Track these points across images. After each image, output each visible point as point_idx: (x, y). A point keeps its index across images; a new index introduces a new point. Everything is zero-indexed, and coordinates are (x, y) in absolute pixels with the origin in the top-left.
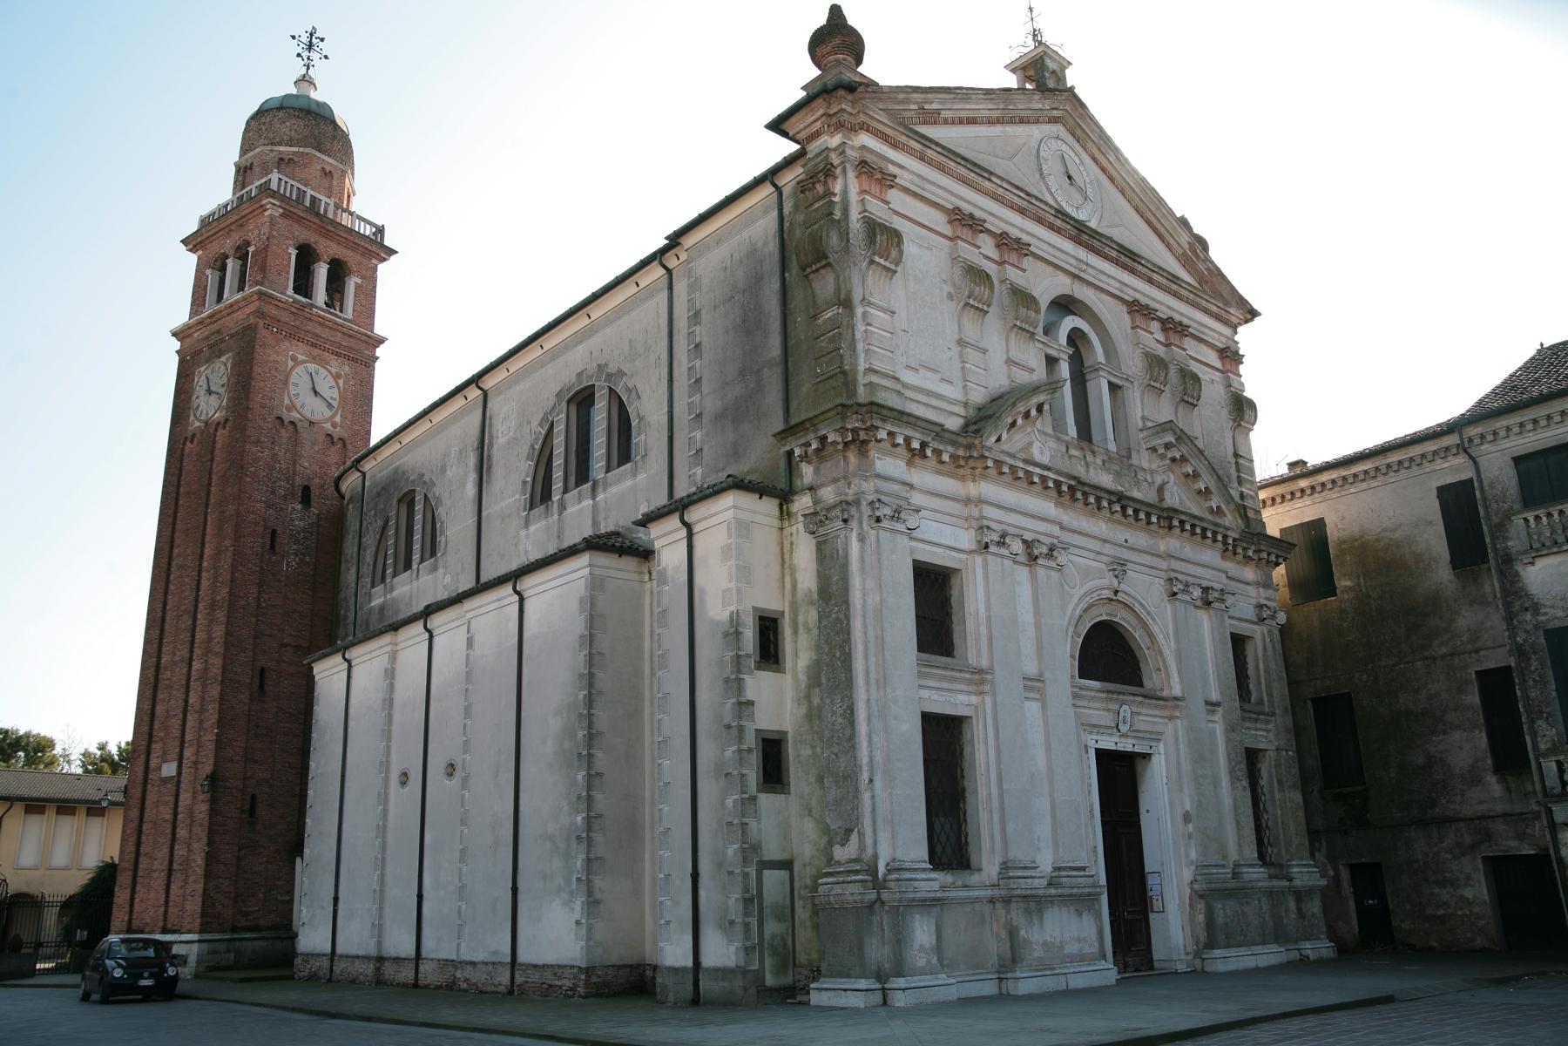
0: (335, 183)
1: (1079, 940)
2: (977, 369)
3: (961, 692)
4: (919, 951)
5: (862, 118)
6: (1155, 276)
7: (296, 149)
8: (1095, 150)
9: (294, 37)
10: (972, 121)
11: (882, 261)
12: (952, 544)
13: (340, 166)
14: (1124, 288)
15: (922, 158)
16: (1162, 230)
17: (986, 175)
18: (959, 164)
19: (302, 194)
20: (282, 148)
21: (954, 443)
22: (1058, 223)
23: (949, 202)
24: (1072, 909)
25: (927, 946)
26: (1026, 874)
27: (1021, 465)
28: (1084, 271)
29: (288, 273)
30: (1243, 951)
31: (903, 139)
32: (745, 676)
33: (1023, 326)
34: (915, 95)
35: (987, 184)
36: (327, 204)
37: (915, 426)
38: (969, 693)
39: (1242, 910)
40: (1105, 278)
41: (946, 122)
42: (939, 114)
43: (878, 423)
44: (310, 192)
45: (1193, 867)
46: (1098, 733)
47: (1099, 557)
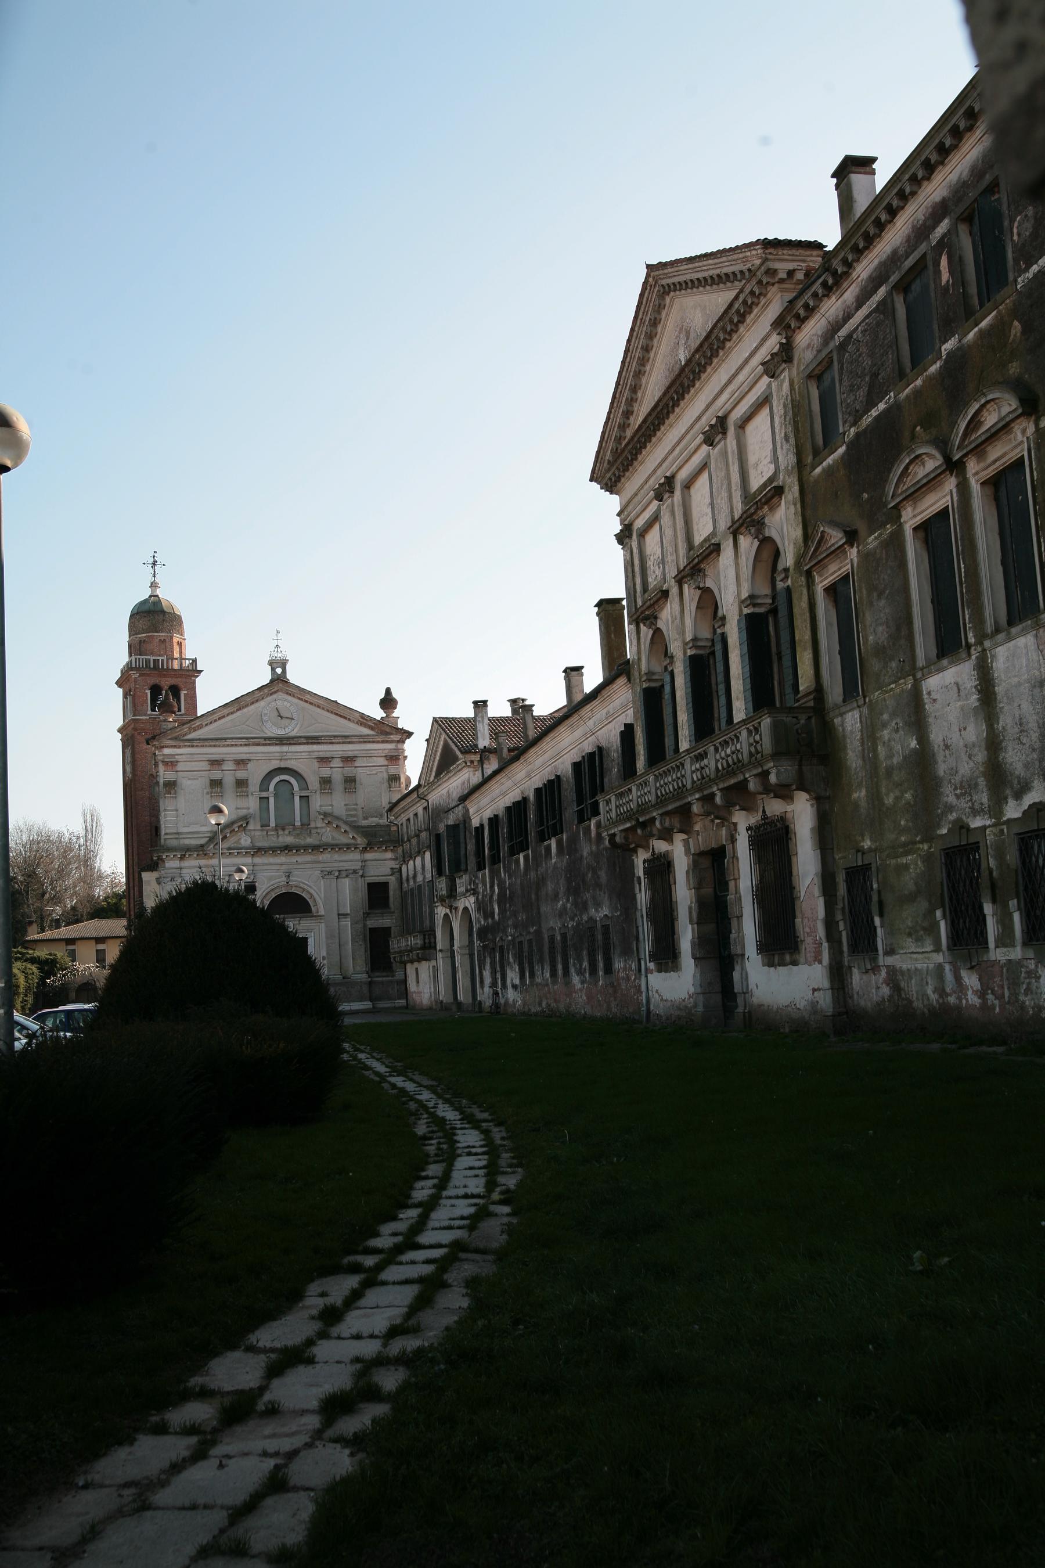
0: (167, 644)
7: (145, 635)
9: (144, 564)
10: (223, 717)
13: (169, 634)
14: (312, 754)
19: (148, 661)
20: (140, 636)
22: (268, 742)
29: (147, 703)
31: (182, 744)
35: (226, 743)
36: (162, 660)
37: (176, 851)
40: (299, 754)
41: (207, 725)
44: (152, 658)
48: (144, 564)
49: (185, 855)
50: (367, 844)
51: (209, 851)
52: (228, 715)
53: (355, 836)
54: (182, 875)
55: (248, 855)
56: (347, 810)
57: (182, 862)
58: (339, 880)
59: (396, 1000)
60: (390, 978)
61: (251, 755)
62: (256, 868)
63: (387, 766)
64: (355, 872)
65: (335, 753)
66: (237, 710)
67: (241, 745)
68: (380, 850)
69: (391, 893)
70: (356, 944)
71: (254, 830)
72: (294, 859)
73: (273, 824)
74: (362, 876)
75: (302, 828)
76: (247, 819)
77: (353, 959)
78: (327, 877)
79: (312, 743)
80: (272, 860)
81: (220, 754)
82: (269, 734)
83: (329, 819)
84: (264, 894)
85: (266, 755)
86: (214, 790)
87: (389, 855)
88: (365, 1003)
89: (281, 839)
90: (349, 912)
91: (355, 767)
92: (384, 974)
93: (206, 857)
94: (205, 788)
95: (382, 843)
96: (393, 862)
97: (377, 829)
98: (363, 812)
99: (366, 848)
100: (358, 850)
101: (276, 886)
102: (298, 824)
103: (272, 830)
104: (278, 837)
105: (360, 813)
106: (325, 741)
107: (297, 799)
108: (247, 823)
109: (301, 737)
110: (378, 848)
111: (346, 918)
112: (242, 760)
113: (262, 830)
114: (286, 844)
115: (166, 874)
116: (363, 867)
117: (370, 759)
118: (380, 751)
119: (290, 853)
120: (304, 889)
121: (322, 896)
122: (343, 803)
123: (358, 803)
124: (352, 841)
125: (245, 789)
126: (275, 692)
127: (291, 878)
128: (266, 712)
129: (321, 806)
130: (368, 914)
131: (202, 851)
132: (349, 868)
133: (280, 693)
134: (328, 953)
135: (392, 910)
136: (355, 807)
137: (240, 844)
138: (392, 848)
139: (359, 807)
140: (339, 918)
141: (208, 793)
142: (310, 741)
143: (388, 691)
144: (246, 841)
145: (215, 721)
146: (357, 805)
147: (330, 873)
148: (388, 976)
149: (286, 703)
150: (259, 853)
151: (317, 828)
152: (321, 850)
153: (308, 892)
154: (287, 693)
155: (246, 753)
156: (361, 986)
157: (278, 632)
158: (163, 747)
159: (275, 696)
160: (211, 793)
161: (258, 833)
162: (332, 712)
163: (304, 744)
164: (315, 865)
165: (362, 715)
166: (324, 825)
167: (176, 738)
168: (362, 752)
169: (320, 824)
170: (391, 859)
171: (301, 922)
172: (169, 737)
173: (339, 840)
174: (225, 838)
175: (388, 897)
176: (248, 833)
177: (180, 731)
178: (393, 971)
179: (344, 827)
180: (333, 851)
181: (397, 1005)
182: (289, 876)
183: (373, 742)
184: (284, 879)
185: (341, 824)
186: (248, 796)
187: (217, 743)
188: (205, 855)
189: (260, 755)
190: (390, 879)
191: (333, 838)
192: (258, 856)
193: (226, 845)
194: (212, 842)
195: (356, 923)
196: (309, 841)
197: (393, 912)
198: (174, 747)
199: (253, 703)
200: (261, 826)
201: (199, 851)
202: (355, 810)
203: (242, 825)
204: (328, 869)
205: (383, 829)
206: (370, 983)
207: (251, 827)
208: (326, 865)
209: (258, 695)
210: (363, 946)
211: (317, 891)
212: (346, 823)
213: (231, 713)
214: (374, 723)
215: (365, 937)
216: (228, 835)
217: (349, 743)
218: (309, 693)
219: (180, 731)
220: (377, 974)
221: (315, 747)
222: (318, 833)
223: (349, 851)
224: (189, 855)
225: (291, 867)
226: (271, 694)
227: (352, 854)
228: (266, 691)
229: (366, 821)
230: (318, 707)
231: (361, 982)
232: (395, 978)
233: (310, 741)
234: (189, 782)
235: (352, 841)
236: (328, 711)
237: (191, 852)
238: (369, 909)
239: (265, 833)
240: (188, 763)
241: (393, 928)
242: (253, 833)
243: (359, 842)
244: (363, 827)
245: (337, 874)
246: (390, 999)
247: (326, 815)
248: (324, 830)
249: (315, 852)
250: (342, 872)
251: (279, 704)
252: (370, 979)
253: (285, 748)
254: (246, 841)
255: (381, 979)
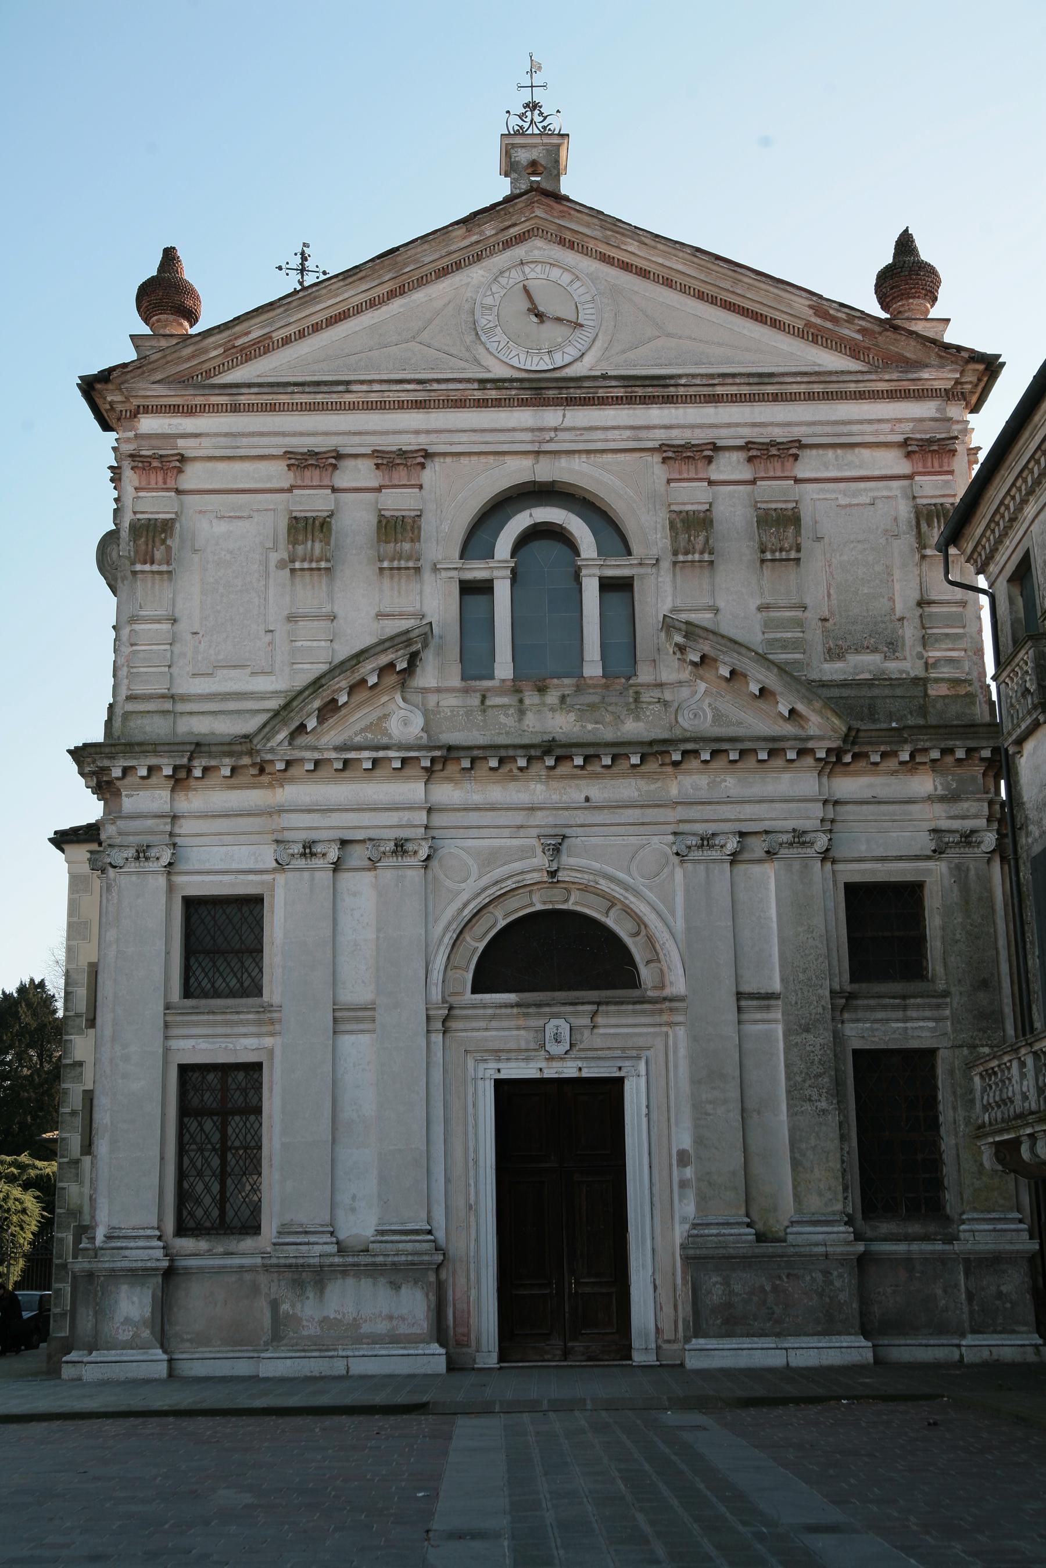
1: (391, 1318)
2: (315, 644)
3: (245, 1035)
4: (122, 1324)
5: (135, 402)
6: (719, 390)
8: (603, 248)
9: (280, 268)
11: (147, 567)
12: (251, 866)
14: (643, 434)
15: (235, 409)
16: (757, 308)
17: (341, 388)
18: (293, 393)
21: (230, 754)
22: (493, 394)
23: (277, 445)
24: (382, 1280)
25: (137, 1318)
26: (299, 1240)
27: (333, 755)
28: (551, 440)
30: (769, 1342)
31: (199, 400)
32: (72, 1037)
33: (395, 564)
34: (211, 340)
35: (349, 398)
37: (155, 753)
38: (259, 1035)
39: (775, 1289)
40: (599, 435)
41: (287, 341)
42: (271, 338)
43: (106, 763)
45: (687, 1227)
46: (499, 1060)
47: (522, 832)
48: (280, 268)
49: (189, 771)
50: (845, 739)
51: (272, 750)
52: (358, 310)
53: (800, 707)
54: (177, 840)
55: (408, 771)
56: (768, 625)
57: (181, 796)
58: (741, 868)
59: (963, 1335)
60: (939, 1247)
61: (433, 438)
62: (438, 820)
63: (910, 477)
64: (799, 838)
65: (724, 432)
66: (392, 295)
67: (401, 406)
68: (892, 764)
69: (933, 922)
70: (807, 1106)
71: (438, 690)
72: (575, 792)
73: (504, 668)
74: (826, 856)
75: (606, 687)
76: (409, 642)
77: (795, 1164)
78: (696, 854)
79: (646, 401)
80: (497, 792)
81: (326, 434)
82: (500, 371)
83: (706, 647)
84: (467, 912)
85: (488, 437)
86: (300, 549)
87: (924, 784)
88: (846, 1341)
89: (531, 720)
90: (777, 986)
91: (797, 481)
92: (915, 1228)
93: (265, 779)
94: (275, 548)
95: (899, 736)
96: (939, 809)
97: (876, 692)
98: (825, 631)
99: (839, 753)
100: (809, 761)
101: (510, 884)
102: (593, 669)
103: (501, 691)
104: (522, 712)
105: (815, 636)
106: (692, 391)
107: (591, 589)
108: (414, 659)
109: (604, 377)
110: (884, 755)
111: (768, 1008)
112: (402, 453)
113: (466, 691)
114: (546, 738)
115: (120, 834)
116: (829, 825)
117: (850, 456)
118: (886, 427)
119: (564, 769)
120: (612, 902)
121: (680, 925)
122: (754, 603)
123: (808, 601)
124: (788, 729)
125: (407, 546)
126: (520, 239)
127: (566, 860)
128: (489, 301)
129: (674, 610)
130: (851, 996)
131: (250, 753)
132: (779, 825)
133: (538, 243)
134: (699, 1141)
135: (941, 986)
136: (798, 614)
137: (386, 733)
138: (935, 754)
139: (811, 616)
140: (739, 1009)
141: (281, 565)
142: (640, 392)
143: (905, 244)
144: (406, 723)
145: (316, 328)
146: (805, 608)
147: (706, 841)
148: (926, 1238)
149: (555, 273)
150: (452, 768)
151: (661, 685)
152: (677, 757)
153: (628, 912)
154: (562, 242)
155: (417, 432)
156: (826, 1273)
157: (534, 68)
158: (135, 414)
159: (519, 252)
160: (293, 561)
161: (450, 701)
162: (713, 301)
163: (618, 401)
164: (651, 814)
165: (819, 304)
166: (686, 674)
167: (184, 381)
168: (818, 429)
169: (671, 671)
170: (930, 799)
171: (600, 1020)
172: (158, 376)
173: (739, 723)
174: (330, 708)
175: (920, 941)
176: (418, 698)
177: (193, 356)
178: (946, 1220)
179: (758, 677)
180: (720, 763)
181: (969, 1357)
182: (557, 850)
183: (860, 396)
184: (541, 860)
185: (746, 664)
186: (417, 570)
187: (319, 398)
188: (262, 771)
189: (464, 437)
190: (929, 871)
191: (718, 717)
192: (449, 779)
193: (333, 735)
194: (285, 722)
195: (807, 1030)
196: (632, 728)
197: (946, 994)
198: (174, 410)
199: (444, 272)
200: (462, 679)
201: (240, 754)
202: (800, 624)
203: (391, 665)
204: (700, 828)
205: (899, 692)
206: (863, 1262)
207: (427, 676)
208: (693, 813)
209: (461, 241)
210: (833, 1119)
211: (661, 907)
212: (762, 658)
213: (373, 304)
214: (862, 331)
215: (838, 1083)
216: (343, 699)
217: (776, 398)
218: (636, 232)
219: (193, 356)
220: (885, 1227)
221: (656, 414)
222: (666, 704)
223: (779, 762)
224: (206, 770)
225: (564, 817)
226: (508, 244)
227: (786, 777)
228: (489, 230)
229: (839, 665)
230: (668, 283)
231: (826, 1256)
232: (957, 1246)
233: (640, 392)
234: (221, 528)
235: (788, 729)
236: (701, 296)
237: (210, 755)
238: (853, 980)
239: (475, 701)
240: (221, 466)
241: (942, 1054)
242: (432, 699)
243: (813, 730)
244: (823, 684)
245: (732, 845)
246: (941, 1329)
247: (691, 631)
248: (685, 692)
249: (652, 766)
250: (751, 841)
251: (533, 272)
252: (860, 1247)
253: (551, 417)
254: (406, 723)
255: (902, 1247)
